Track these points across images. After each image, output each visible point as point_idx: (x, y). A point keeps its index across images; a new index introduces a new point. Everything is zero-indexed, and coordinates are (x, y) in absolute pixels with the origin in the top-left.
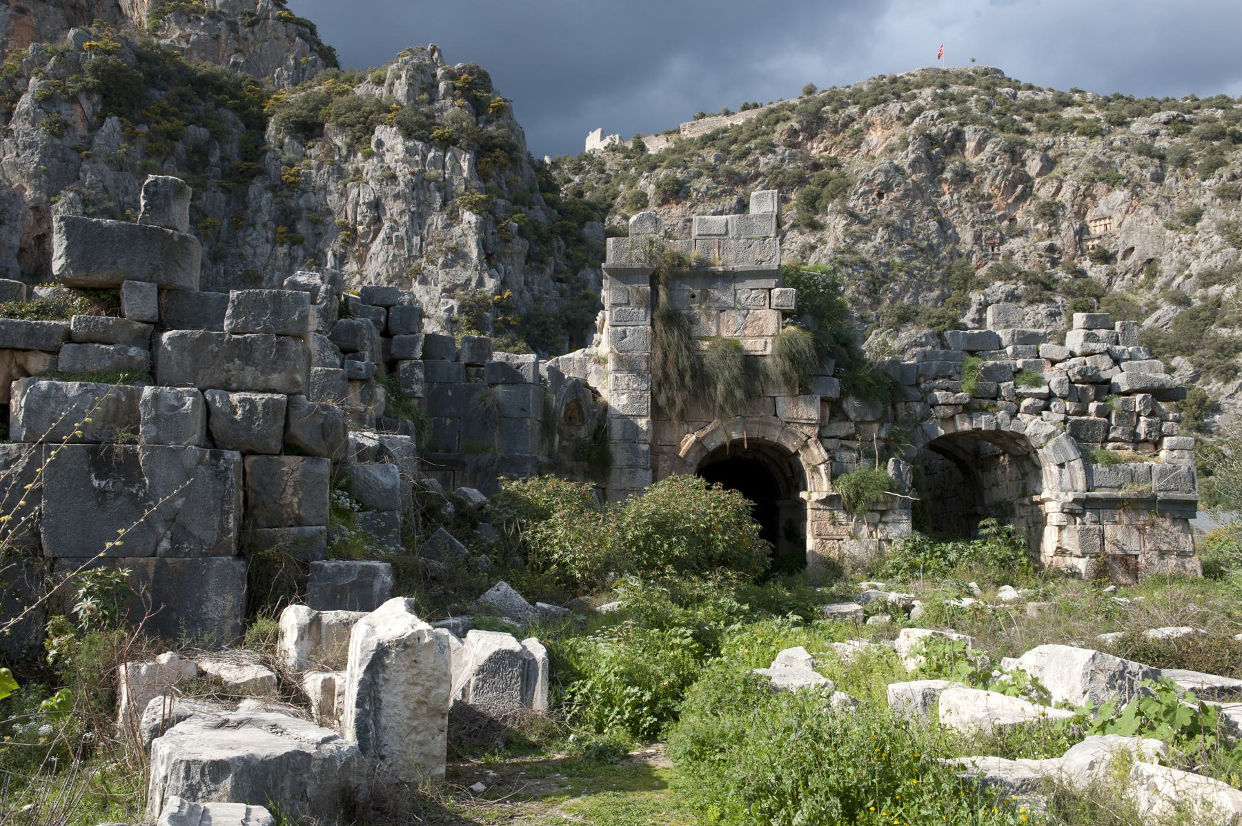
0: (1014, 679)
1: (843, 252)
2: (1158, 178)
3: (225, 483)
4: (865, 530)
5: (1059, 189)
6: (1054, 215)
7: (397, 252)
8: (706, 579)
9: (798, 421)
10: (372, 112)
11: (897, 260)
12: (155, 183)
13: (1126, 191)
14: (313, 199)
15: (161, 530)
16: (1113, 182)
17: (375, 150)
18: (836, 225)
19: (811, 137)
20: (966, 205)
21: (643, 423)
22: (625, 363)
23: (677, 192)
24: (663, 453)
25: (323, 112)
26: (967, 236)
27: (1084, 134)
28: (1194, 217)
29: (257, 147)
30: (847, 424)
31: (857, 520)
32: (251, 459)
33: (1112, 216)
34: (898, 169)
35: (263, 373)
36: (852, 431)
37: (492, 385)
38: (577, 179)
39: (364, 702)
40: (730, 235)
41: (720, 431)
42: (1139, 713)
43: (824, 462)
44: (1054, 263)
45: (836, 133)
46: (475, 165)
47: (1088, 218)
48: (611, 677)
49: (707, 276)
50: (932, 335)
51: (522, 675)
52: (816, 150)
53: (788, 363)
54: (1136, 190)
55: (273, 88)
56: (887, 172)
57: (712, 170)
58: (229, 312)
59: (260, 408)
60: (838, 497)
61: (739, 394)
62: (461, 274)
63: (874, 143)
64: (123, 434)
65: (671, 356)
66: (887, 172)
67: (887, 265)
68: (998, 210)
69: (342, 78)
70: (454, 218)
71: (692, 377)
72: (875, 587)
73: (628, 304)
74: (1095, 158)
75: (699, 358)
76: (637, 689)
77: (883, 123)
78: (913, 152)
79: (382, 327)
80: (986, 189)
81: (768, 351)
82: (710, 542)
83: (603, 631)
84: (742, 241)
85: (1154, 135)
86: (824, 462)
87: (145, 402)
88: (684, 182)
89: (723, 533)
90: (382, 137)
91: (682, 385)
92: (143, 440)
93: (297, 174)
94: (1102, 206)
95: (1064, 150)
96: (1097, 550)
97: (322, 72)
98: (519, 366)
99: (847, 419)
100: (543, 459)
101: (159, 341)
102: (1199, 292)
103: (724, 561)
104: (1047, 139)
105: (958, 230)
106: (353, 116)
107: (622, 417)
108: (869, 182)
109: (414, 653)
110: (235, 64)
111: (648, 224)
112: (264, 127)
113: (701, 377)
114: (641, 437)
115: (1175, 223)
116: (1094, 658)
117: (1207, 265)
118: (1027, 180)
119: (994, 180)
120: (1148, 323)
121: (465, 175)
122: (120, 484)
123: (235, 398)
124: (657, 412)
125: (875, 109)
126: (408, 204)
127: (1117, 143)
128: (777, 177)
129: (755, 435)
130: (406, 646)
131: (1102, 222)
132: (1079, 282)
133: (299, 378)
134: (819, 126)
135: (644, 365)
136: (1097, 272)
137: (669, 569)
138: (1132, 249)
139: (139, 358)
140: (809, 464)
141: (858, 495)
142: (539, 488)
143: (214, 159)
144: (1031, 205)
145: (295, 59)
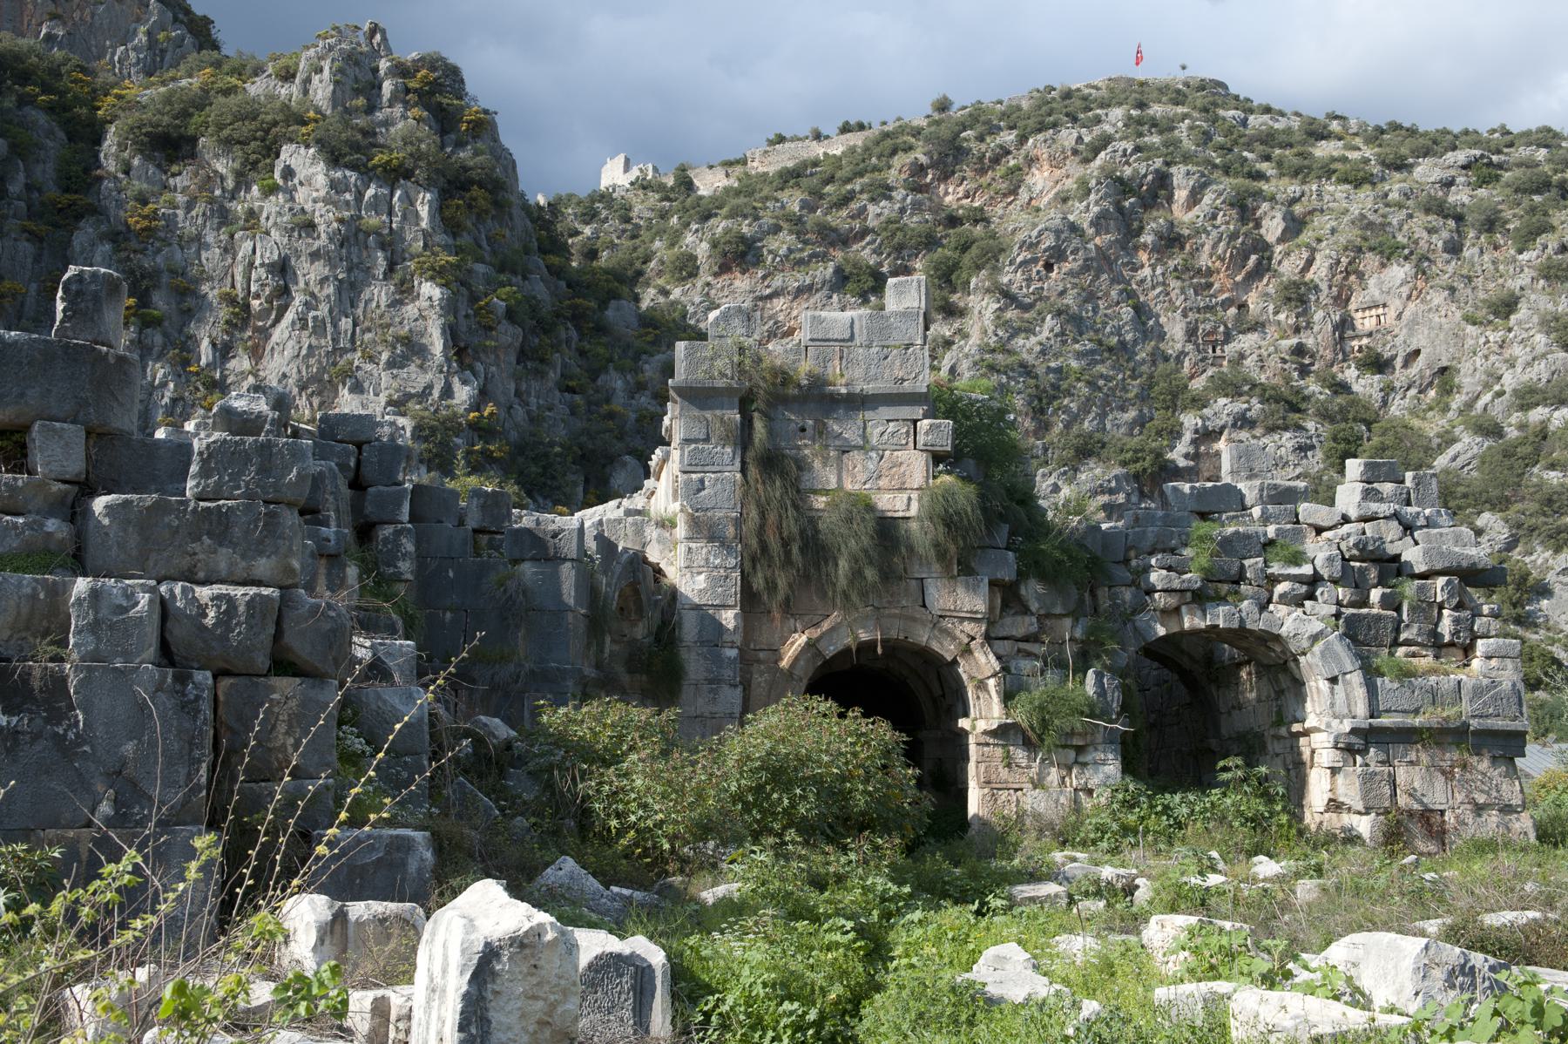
0: (1324, 978)
1: (993, 351)
2: (1454, 249)
3: (195, 718)
4: (1054, 775)
5: (1310, 262)
6: (1303, 301)
7: (314, 342)
8: (845, 849)
9: (955, 613)
10: (275, 124)
11: (1074, 364)
12: (79, 278)
13: (1408, 267)
14: (178, 255)
15: (100, 788)
16: (1389, 252)
17: (280, 182)
18: (982, 310)
19: (945, 177)
20: (1174, 284)
21: (729, 618)
22: (703, 528)
23: (743, 255)
24: (759, 661)
25: (196, 119)
26: (1175, 329)
27: (1346, 181)
28: (1506, 306)
29: (87, 171)
30: (1027, 619)
31: (1043, 760)
32: (226, 682)
33: (1389, 305)
34: (1074, 228)
35: (243, 557)
36: (1034, 628)
37: (516, 562)
38: (588, 231)
39: (469, 1024)
40: (858, 341)
41: (846, 629)
42: (1496, 1013)
43: (994, 676)
44: (1304, 371)
45: (982, 171)
46: (439, 210)
47: (1352, 306)
48: (759, 990)
49: (823, 401)
50: (1126, 477)
51: (633, 988)
52: (952, 195)
53: (941, 529)
54: (1422, 264)
55: (111, 79)
56: (1058, 233)
57: (796, 222)
58: (194, 468)
59: (242, 609)
60: (1015, 726)
61: (870, 574)
62: (416, 378)
63: (1039, 187)
64: (46, 648)
65: (772, 518)
66: (1058, 233)
67: (1059, 370)
68: (1221, 291)
69: (226, 68)
70: (405, 292)
71: (801, 549)
72: (1074, 860)
73: (707, 440)
74: (1363, 216)
75: (813, 522)
76: (796, 1005)
77: (1051, 158)
78: (1097, 203)
79: (351, 475)
80: (1204, 260)
81: (913, 511)
82: (846, 796)
83: (731, 925)
84: (874, 350)
85: (1448, 184)
86: (994, 676)
87: (79, 601)
88: (754, 240)
89: (866, 781)
90: (293, 163)
91: (788, 561)
92: (75, 656)
93: (154, 216)
94: (1373, 290)
95: (1315, 204)
96: (1387, 804)
97: (193, 57)
98: (555, 535)
99: (1026, 611)
100: (590, 672)
101: (88, 512)
102: (1516, 417)
103: (862, 825)
104: (1293, 188)
105: (1163, 320)
106: (245, 129)
107: (697, 607)
108: (1032, 246)
109: (533, 956)
110: (50, 38)
111: (736, 322)
112: (98, 140)
113: (814, 549)
114: (726, 638)
115: (1481, 314)
116: (1427, 947)
117: (1526, 378)
118: (1263, 248)
119: (1215, 246)
120: (1441, 462)
121: (424, 224)
122: (39, 721)
123: (204, 593)
124: (750, 600)
125: (1040, 137)
126: (333, 267)
127: (1394, 196)
128: (894, 235)
129: (893, 634)
130: (522, 946)
131: (1374, 312)
132: (1340, 400)
133: (296, 564)
134: (957, 161)
135: (730, 531)
136: (1366, 386)
137: (791, 835)
138: (1417, 352)
139: (60, 536)
140: (972, 678)
141: (1045, 724)
142: (598, 719)
143: (15, 188)
144: (1268, 285)
145: (149, 33)
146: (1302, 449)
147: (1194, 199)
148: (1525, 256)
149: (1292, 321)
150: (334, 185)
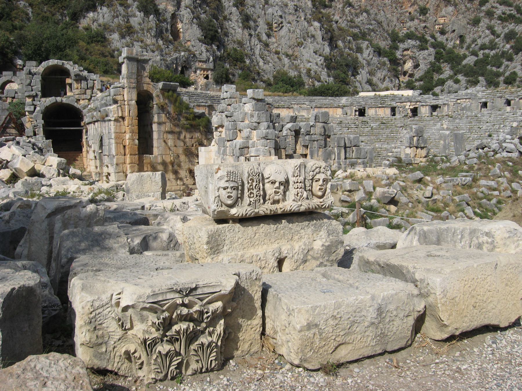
28: (476, 22)
94: (443, 13)
120: (464, 62)
131: (444, 18)
138: (454, 31)
146: (429, 55)
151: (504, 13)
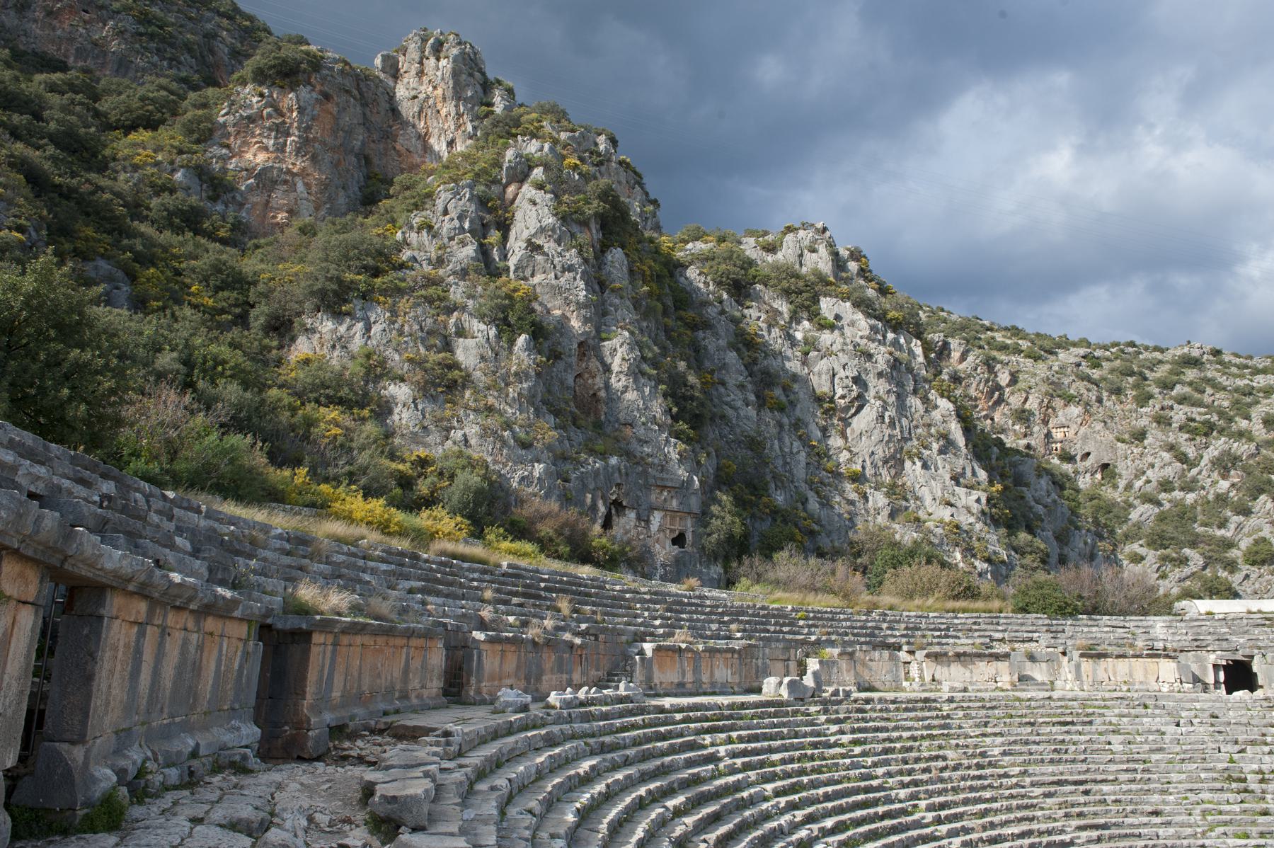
2: (1100, 401)
5: (1026, 399)
16: (1069, 400)
47: (1050, 425)
68: (983, 410)
70: (929, 406)
74: (1048, 379)
85: (1078, 365)
115: (1126, 436)
117: (1161, 474)
118: (999, 388)
138: (1088, 454)
147: (963, 358)
148: (1144, 410)
149: (1023, 430)
150: (872, 328)
151: (1193, 420)
